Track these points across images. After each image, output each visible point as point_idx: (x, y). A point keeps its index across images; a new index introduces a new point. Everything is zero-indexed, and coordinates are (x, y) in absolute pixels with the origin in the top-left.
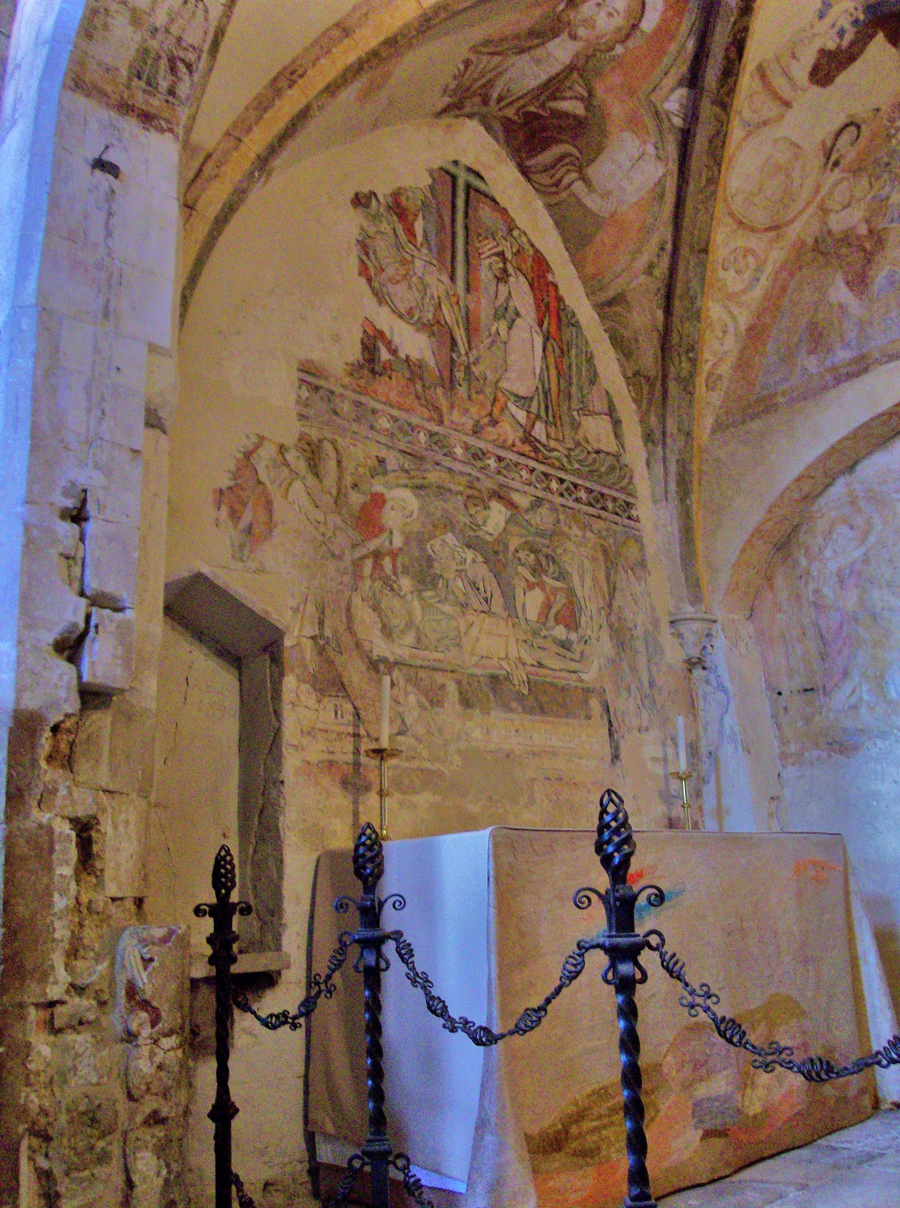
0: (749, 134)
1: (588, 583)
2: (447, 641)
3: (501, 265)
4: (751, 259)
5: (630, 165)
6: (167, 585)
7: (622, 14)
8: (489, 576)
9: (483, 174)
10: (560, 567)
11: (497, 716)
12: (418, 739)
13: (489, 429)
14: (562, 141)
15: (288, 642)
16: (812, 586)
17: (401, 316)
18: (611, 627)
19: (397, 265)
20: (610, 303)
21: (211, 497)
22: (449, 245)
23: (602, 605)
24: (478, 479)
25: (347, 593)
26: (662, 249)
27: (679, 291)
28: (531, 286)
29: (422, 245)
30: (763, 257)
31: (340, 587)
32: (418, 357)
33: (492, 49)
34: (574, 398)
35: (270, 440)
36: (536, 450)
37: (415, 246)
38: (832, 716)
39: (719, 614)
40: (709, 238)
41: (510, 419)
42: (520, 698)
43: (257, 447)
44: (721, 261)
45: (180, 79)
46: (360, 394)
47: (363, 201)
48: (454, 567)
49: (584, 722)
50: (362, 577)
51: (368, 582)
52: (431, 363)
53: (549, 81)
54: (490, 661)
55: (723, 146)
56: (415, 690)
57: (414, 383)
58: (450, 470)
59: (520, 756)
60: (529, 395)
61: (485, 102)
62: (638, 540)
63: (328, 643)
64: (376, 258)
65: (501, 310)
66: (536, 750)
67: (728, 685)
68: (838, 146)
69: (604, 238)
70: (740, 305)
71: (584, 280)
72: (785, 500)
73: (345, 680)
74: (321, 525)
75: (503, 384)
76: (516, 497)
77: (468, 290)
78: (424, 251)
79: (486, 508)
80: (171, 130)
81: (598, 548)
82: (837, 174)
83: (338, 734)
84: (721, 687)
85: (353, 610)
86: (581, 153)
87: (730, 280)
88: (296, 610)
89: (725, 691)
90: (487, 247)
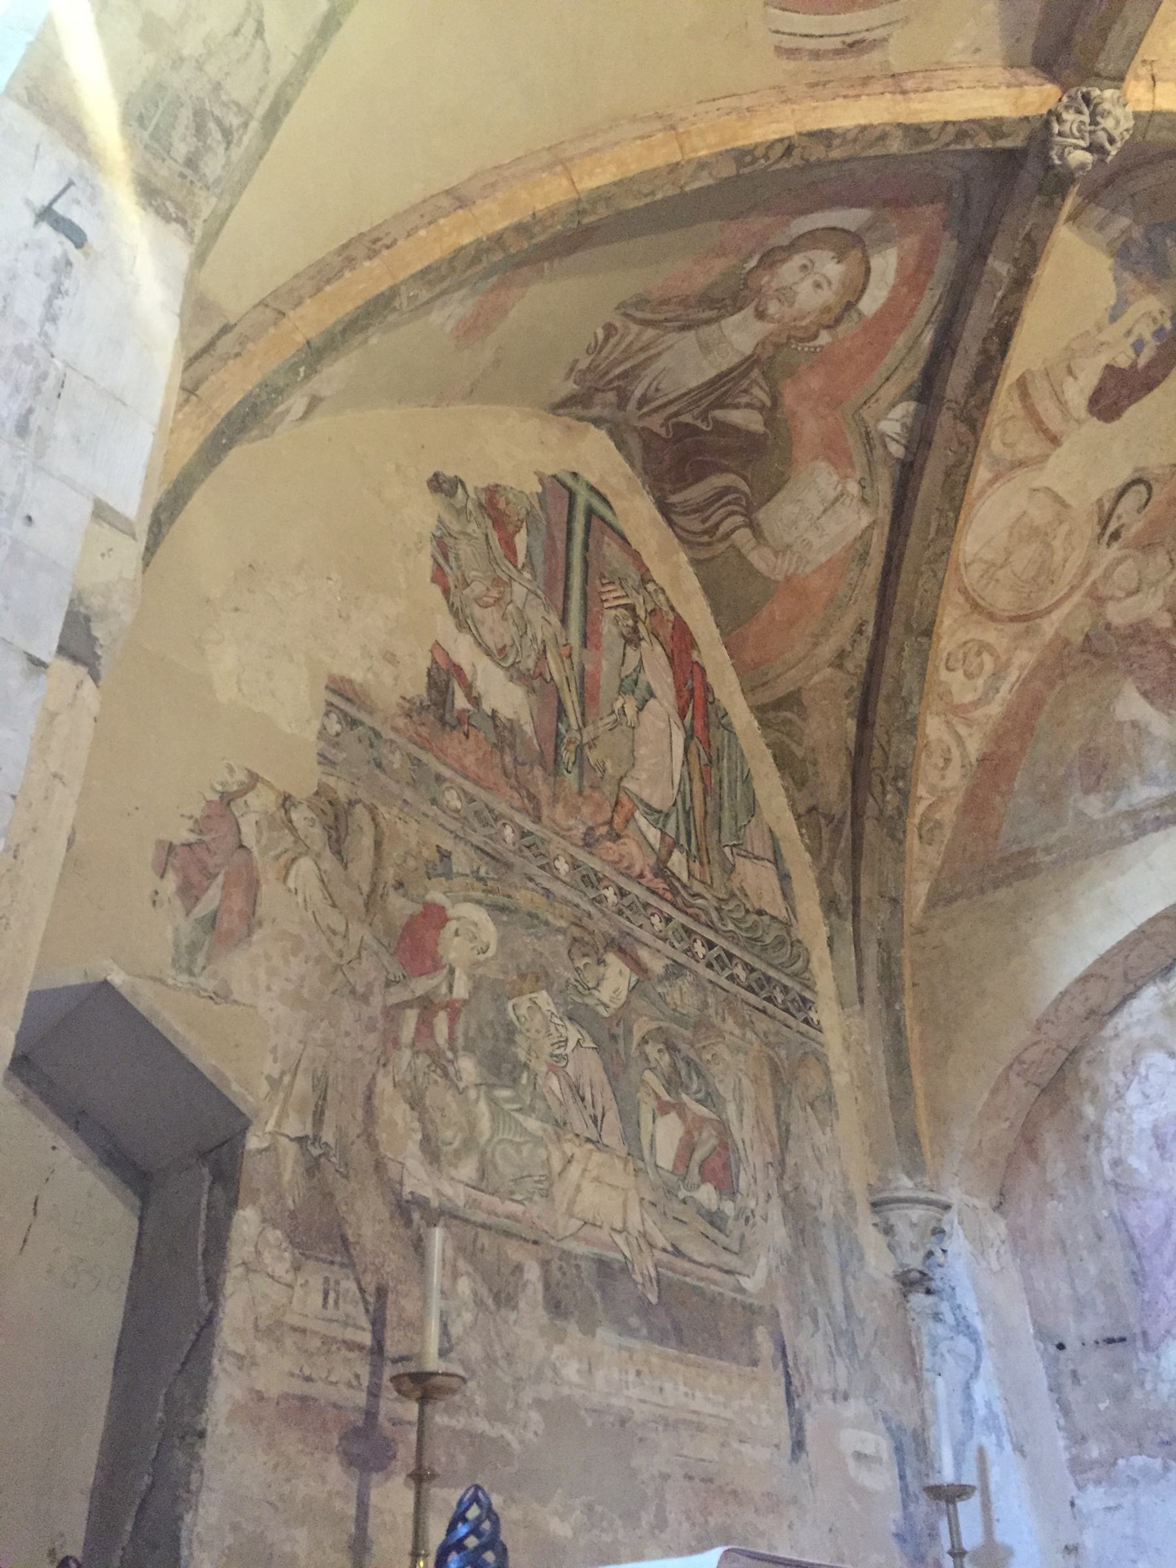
0: (996, 478)
1: (748, 1120)
2: (529, 1184)
3: (630, 622)
4: (986, 657)
5: (821, 508)
6: (34, 997)
7: (834, 287)
8: (600, 1077)
9: (610, 498)
10: (707, 1084)
11: (606, 1336)
13: (608, 844)
14: (726, 470)
15: (253, 1142)
16: (1107, 1155)
17: (488, 653)
18: (784, 1197)
19: (488, 583)
20: (778, 705)
21: (149, 853)
24: (589, 915)
26: (860, 632)
27: (886, 688)
28: (671, 659)
29: (523, 567)
30: (1004, 658)
31: (360, 1055)
32: (511, 716)
33: (648, 316)
34: (726, 830)
37: (515, 567)
39: (954, 1194)
40: (935, 614)
43: (245, 789)
44: (945, 656)
45: (208, 148)
46: (422, 748)
47: (445, 486)
49: (749, 1369)
50: (396, 1043)
51: (407, 1054)
52: (529, 729)
53: (720, 376)
54: (598, 1231)
55: (966, 482)
56: (471, 1270)
57: (502, 751)
58: (547, 893)
60: (665, 810)
62: (821, 1059)
64: (459, 567)
65: (627, 682)
67: (977, 1323)
68: (1115, 514)
70: (969, 723)
71: (741, 669)
72: (1062, 1007)
73: (350, 1233)
74: (339, 938)
75: (628, 784)
76: (644, 955)
77: (584, 644)
78: (527, 575)
79: (601, 962)
80: (184, 223)
82: (1115, 551)
83: (327, 1340)
84: (964, 1327)
85: (376, 1102)
86: (751, 487)
89: (973, 1336)
90: (613, 594)
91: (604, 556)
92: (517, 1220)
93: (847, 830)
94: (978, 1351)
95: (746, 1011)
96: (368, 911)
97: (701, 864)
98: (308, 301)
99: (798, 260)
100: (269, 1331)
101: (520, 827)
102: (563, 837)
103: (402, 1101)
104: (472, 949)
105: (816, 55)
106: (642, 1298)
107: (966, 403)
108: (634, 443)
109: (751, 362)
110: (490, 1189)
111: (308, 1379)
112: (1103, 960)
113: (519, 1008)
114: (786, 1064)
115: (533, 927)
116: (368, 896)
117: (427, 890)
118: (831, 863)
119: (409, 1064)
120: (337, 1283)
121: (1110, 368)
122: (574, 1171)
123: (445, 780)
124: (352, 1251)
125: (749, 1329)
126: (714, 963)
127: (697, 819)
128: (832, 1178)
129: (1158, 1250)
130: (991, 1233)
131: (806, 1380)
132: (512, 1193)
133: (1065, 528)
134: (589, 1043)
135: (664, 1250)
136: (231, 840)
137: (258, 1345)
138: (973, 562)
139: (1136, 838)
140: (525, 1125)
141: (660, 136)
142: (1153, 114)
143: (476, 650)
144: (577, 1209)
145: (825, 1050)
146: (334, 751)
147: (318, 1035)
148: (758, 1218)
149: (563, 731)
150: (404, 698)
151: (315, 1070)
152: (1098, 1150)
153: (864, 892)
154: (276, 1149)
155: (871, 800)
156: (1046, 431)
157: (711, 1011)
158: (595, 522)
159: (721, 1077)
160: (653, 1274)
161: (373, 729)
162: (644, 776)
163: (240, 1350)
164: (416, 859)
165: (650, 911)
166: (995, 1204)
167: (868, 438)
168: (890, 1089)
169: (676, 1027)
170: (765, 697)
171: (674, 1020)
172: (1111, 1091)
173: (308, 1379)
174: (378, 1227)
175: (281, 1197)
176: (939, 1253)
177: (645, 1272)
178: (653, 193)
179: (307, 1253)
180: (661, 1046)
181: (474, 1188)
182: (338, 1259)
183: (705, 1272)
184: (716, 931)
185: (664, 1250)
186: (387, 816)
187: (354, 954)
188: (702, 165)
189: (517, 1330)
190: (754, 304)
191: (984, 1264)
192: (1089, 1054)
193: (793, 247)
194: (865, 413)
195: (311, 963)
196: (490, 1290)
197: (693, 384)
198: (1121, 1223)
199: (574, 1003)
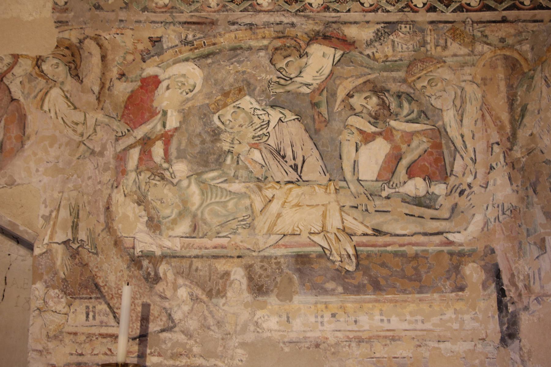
12: (188, 334)
23: (495, 137)
24: (293, 25)
25: (106, 192)
35: (27, 57)
48: (251, 135)
51: (133, 175)
54: (296, 238)
58: (251, 26)
59: (337, 344)
63: (82, 246)
66: (365, 335)
76: (351, 32)
85: (113, 208)
88: (47, 218)
92: (223, 247)
100: (56, 337)
103: (131, 203)
104: (181, 93)
111: (81, 355)
115: (237, 55)
116: (99, 93)
117: (143, 70)
119: (135, 181)
120: (94, 307)
122: (275, 207)
124: (102, 288)
131: (524, 291)
132: (218, 233)
134: (290, 116)
135: (365, 235)
136: (6, 99)
137: (49, 344)
144: (276, 229)
146: (65, 15)
147: (70, 185)
151: (70, 205)
154: (50, 250)
160: (351, 252)
163: (40, 348)
164: (132, 54)
169: (385, 74)
171: (386, 69)
173: (81, 355)
175: (56, 273)
177: (343, 252)
179: (74, 297)
181: (187, 237)
182: (94, 296)
183: (406, 240)
185: (365, 235)
186: (107, 37)
187: (91, 131)
189: (226, 308)
195: (62, 148)
196: (204, 290)
199: (276, 94)
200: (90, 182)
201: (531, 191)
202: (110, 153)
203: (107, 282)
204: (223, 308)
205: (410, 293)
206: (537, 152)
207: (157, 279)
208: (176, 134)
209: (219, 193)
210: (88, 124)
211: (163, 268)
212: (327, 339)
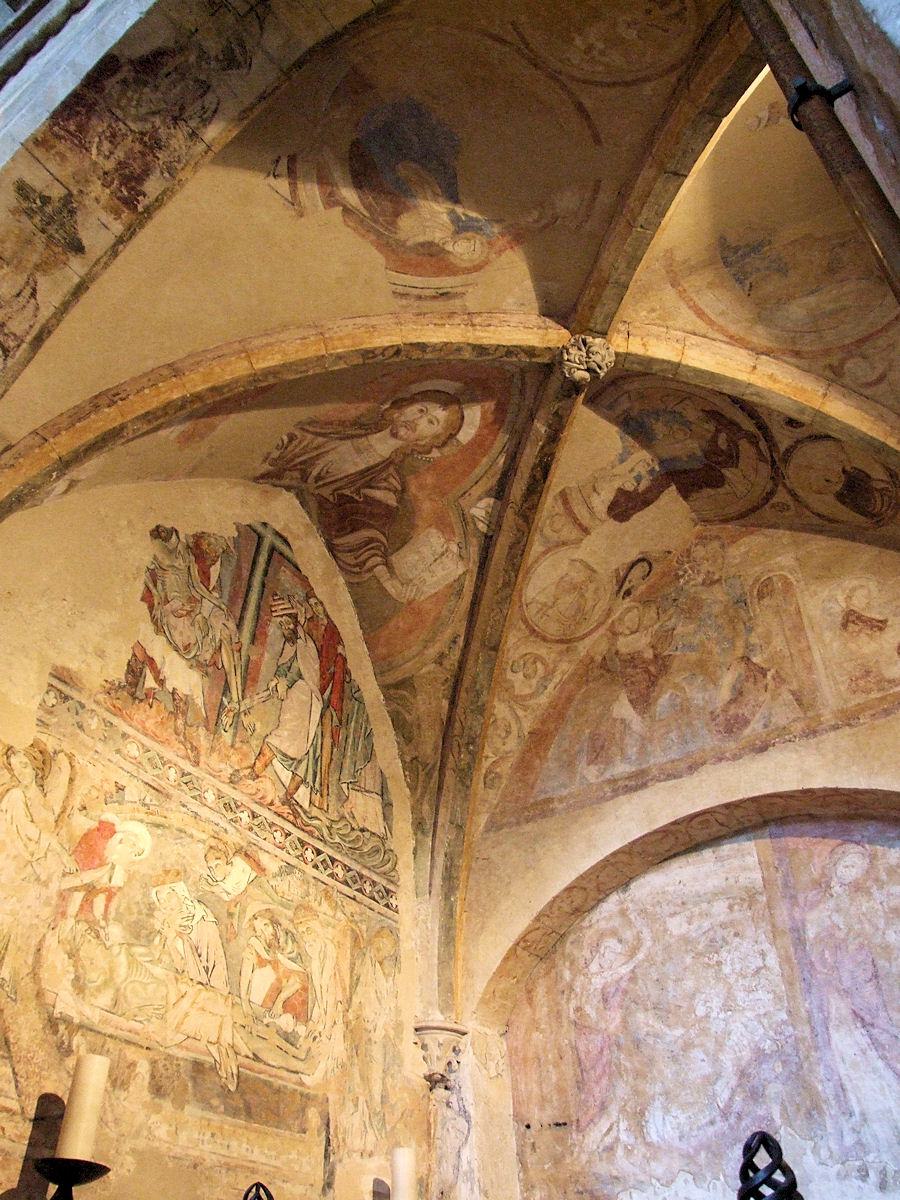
3: (292, 626)
9: (290, 540)
11: (192, 1111)
13: (250, 782)
14: (371, 527)
16: (573, 1004)
17: (177, 650)
18: (347, 1024)
20: (401, 684)
22: (242, 595)
26: (455, 642)
27: (466, 682)
30: (551, 666)
31: (36, 921)
34: (345, 771)
36: (296, 814)
38: (584, 1158)
39: (470, 1024)
41: (274, 778)
42: (225, 1093)
48: (179, 921)
49: (298, 1135)
50: (64, 914)
51: (71, 922)
55: (522, 555)
61: (304, 478)
62: (393, 932)
67: (471, 1110)
68: (629, 577)
69: (401, 622)
72: (555, 909)
75: (273, 741)
76: (264, 859)
77: (253, 640)
78: (216, 595)
81: (349, 932)
85: (44, 952)
87: (519, 682)
90: (281, 607)
91: (279, 580)
92: (137, 1033)
93: (436, 774)
94: (469, 1129)
95: (338, 898)
96: (57, 826)
97: (321, 795)
98: (64, 433)
99: (416, 407)
101: (182, 770)
102: (214, 777)
105: (419, 298)
106: (224, 1087)
107: (522, 505)
108: (313, 504)
109: (388, 463)
110: (120, 1013)
112: (582, 877)
113: (162, 895)
114: (365, 935)
116: (59, 816)
118: (423, 795)
121: (621, 491)
122: (185, 1004)
123: (129, 736)
125: (303, 1110)
126: (319, 864)
127: (324, 764)
128: (387, 1012)
129: (593, 1068)
130: (495, 1052)
133: (592, 587)
135: (247, 1057)
138: (531, 603)
139: (612, 798)
140: (152, 971)
141: (312, 338)
142: (628, 354)
143: (168, 647)
144: (183, 1028)
145: (398, 926)
148: (323, 1038)
149: (226, 703)
150: (106, 681)
152: (568, 1000)
153: (441, 820)
155: (451, 756)
156: (580, 525)
157: (311, 898)
158: (276, 555)
159: (313, 943)
160: (235, 1072)
161: (80, 703)
162: (286, 733)
164: (99, 790)
165: (274, 828)
166: (502, 1032)
167: (464, 519)
168: (439, 954)
169: (281, 909)
170: (390, 679)
172: (582, 962)
174: (33, 1034)
176: (455, 1063)
177: (229, 1070)
178: (307, 371)
180: (267, 921)
184: (325, 842)
185: (247, 1057)
186: (81, 761)
187: (42, 854)
188: (340, 357)
189: (126, 1103)
190: (388, 430)
191: (484, 1072)
192: (572, 937)
193: (412, 400)
194: (463, 502)
197: (352, 471)
198: (575, 1049)
200: (28, 912)
201: (355, 1051)
202: (54, 887)
203: (18, 1039)
204: (124, 1103)
205: (271, 1126)
206: (361, 1018)
207: (69, 1052)
208: (118, 893)
209: (143, 972)
210: (42, 845)
211: (77, 1040)
212: (204, 1160)
